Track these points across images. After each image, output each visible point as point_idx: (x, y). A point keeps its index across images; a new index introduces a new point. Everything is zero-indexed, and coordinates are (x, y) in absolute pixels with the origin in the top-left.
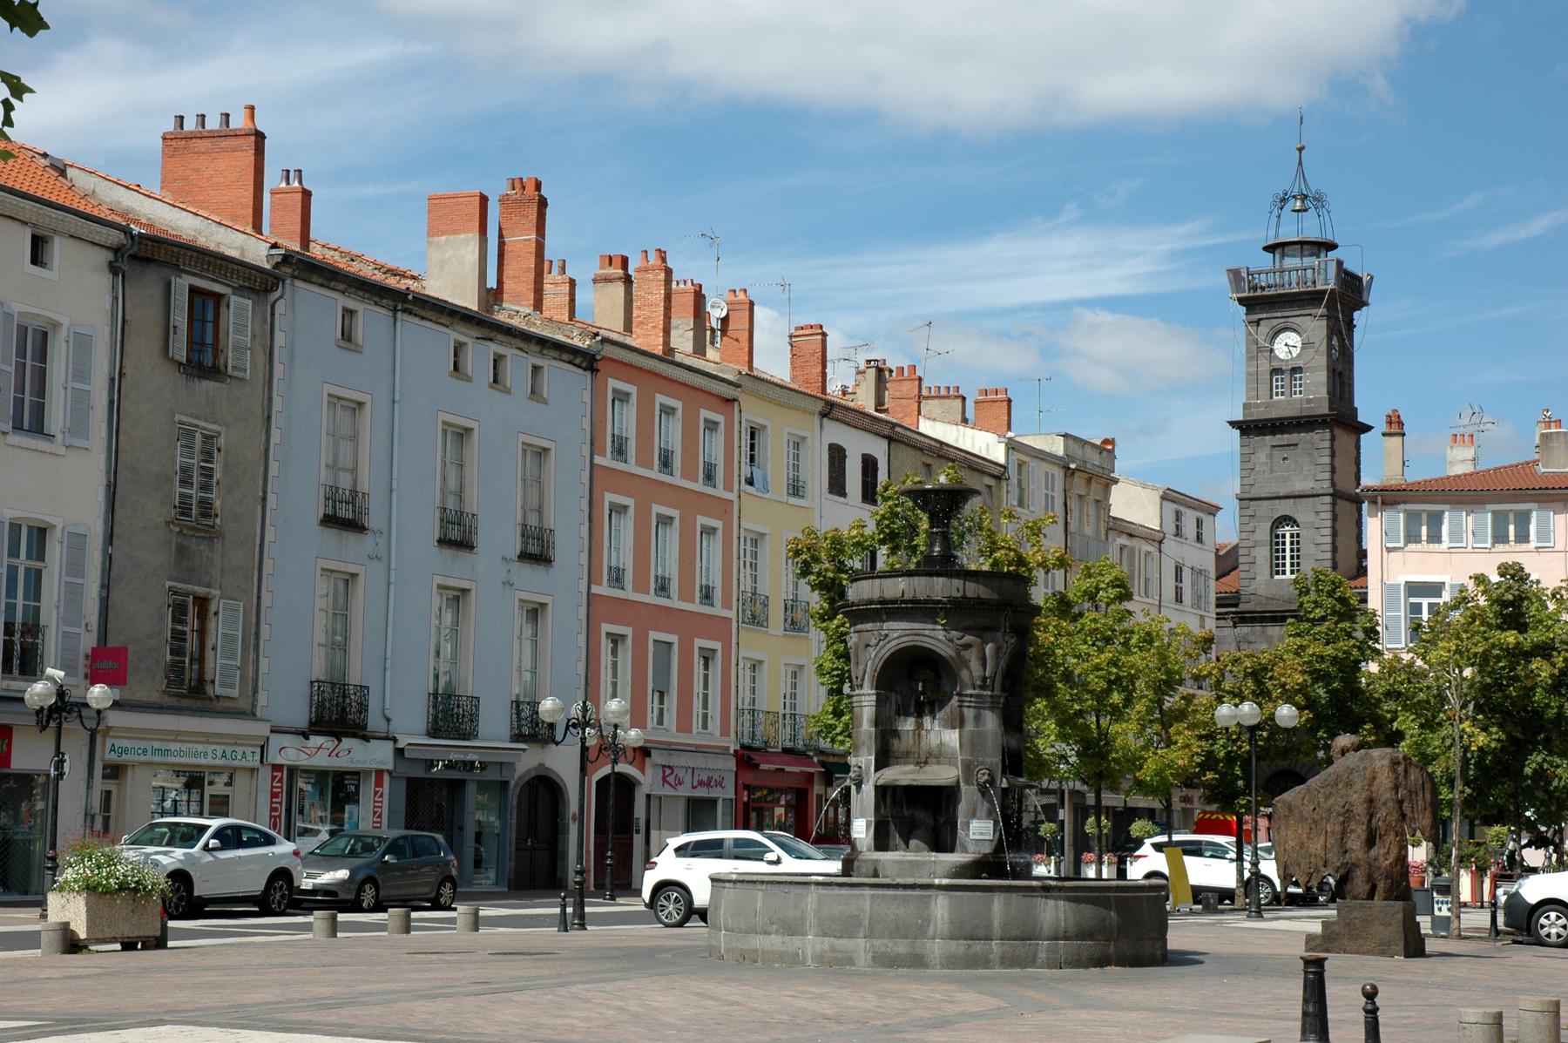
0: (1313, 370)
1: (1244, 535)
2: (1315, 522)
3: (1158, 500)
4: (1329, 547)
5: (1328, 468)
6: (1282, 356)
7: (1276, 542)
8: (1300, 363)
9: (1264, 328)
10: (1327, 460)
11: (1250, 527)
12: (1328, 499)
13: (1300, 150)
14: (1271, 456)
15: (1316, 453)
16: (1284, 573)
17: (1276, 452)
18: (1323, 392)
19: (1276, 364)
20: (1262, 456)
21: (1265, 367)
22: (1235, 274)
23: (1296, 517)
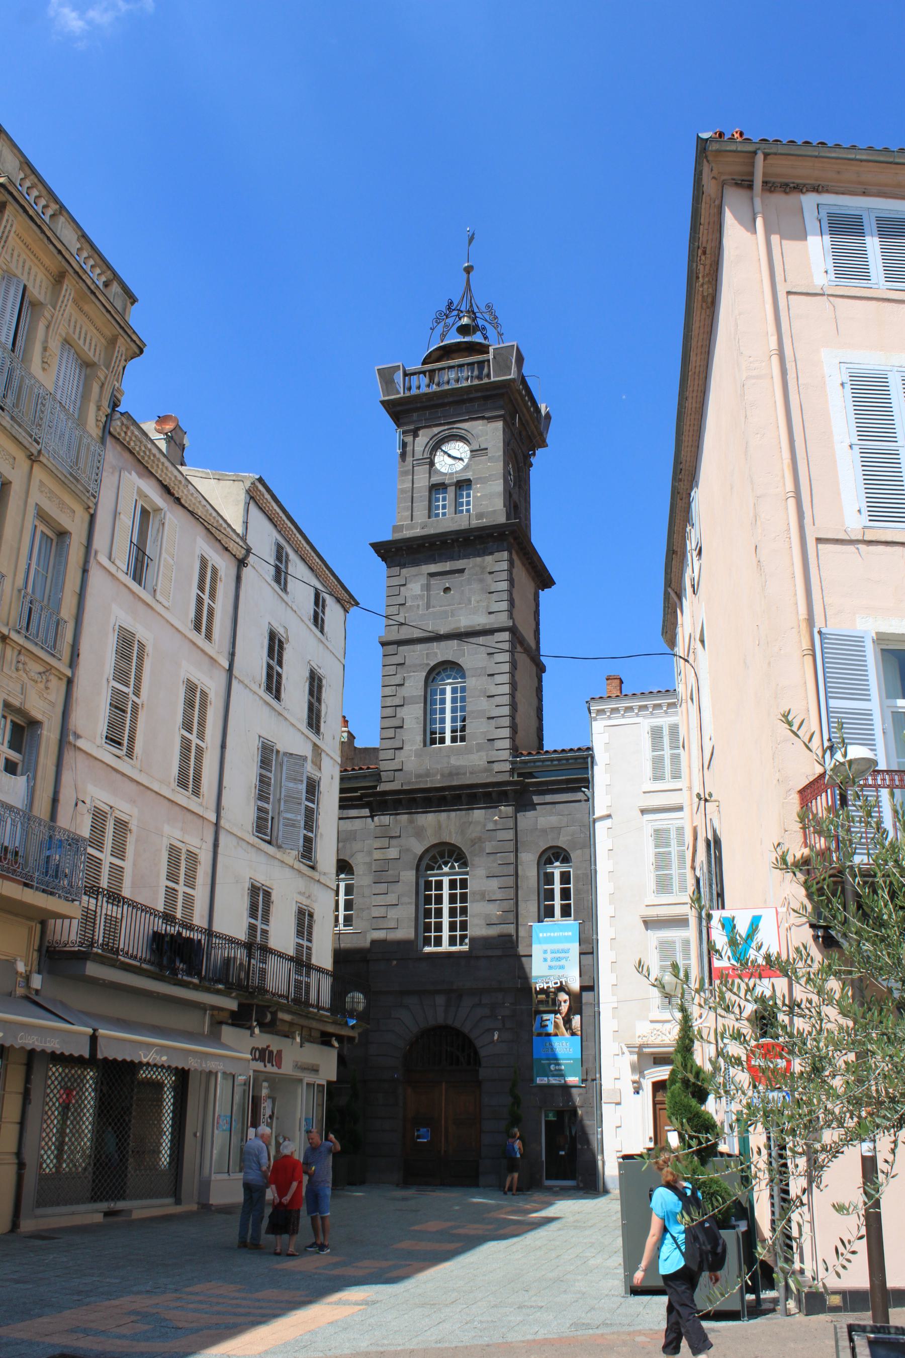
0: (483, 480)
1: (389, 691)
2: (486, 672)
3: (242, 496)
4: (506, 700)
5: (505, 596)
6: (443, 470)
7: (429, 700)
8: (469, 475)
9: (423, 439)
10: (504, 585)
11: (397, 680)
12: (506, 636)
13: (468, 270)
14: (428, 587)
15: (489, 578)
16: (442, 741)
17: (434, 581)
18: (498, 504)
19: (435, 479)
20: (415, 588)
21: (422, 481)
22: (386, 376)
23: (460, 662)
